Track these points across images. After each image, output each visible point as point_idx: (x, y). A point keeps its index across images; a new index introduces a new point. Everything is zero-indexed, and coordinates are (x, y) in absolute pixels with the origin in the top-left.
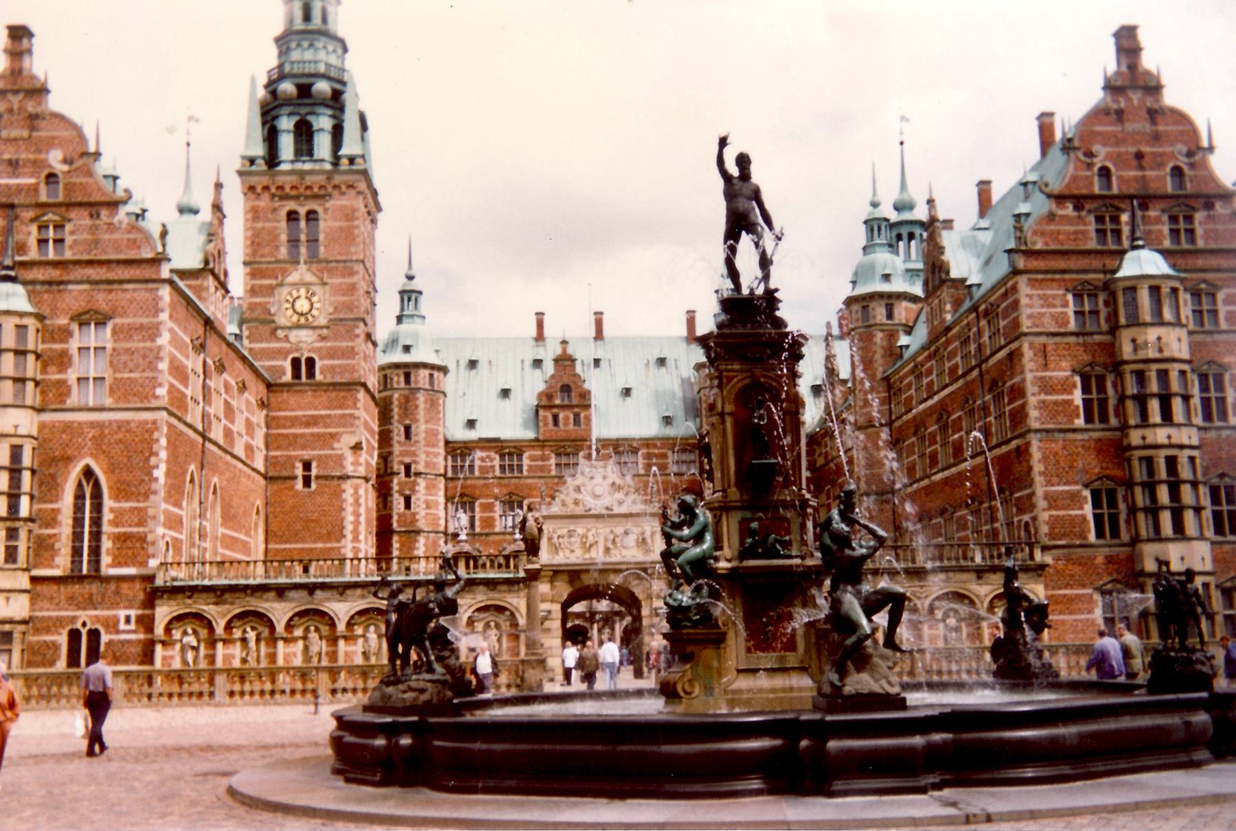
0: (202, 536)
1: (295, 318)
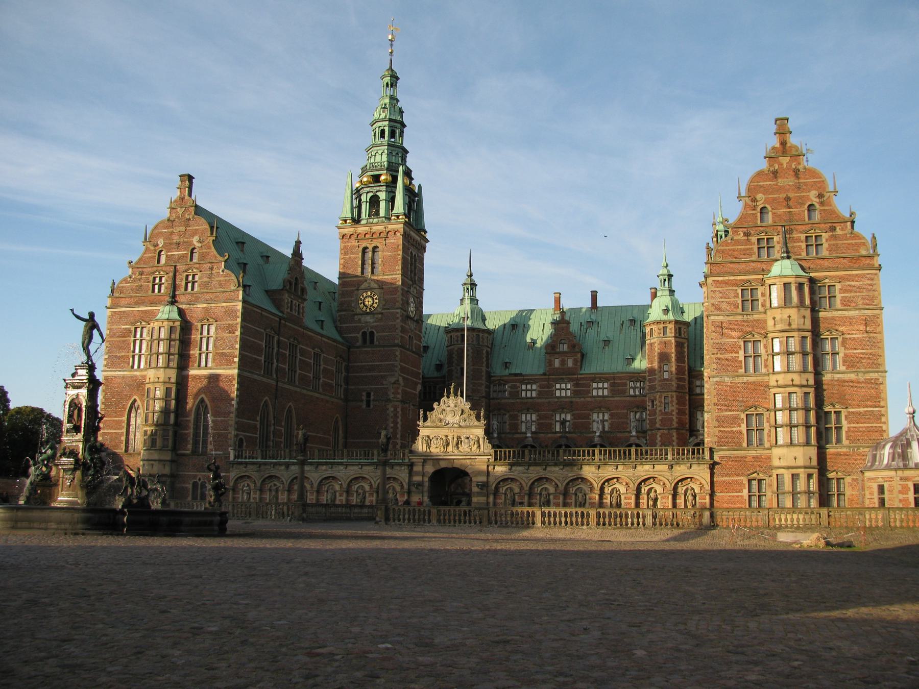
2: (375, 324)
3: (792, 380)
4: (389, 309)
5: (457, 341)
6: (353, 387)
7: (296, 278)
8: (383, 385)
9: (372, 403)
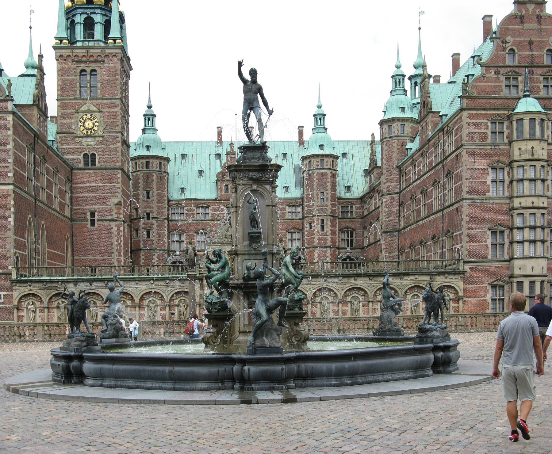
0: (37, 253)
1: (85, 131)
3: (533, 203)
4: (109, 132)
5: (143, 167)
6: (78, 207)
7: (41, 93)
8: (107, 205)
9: (96, 222)
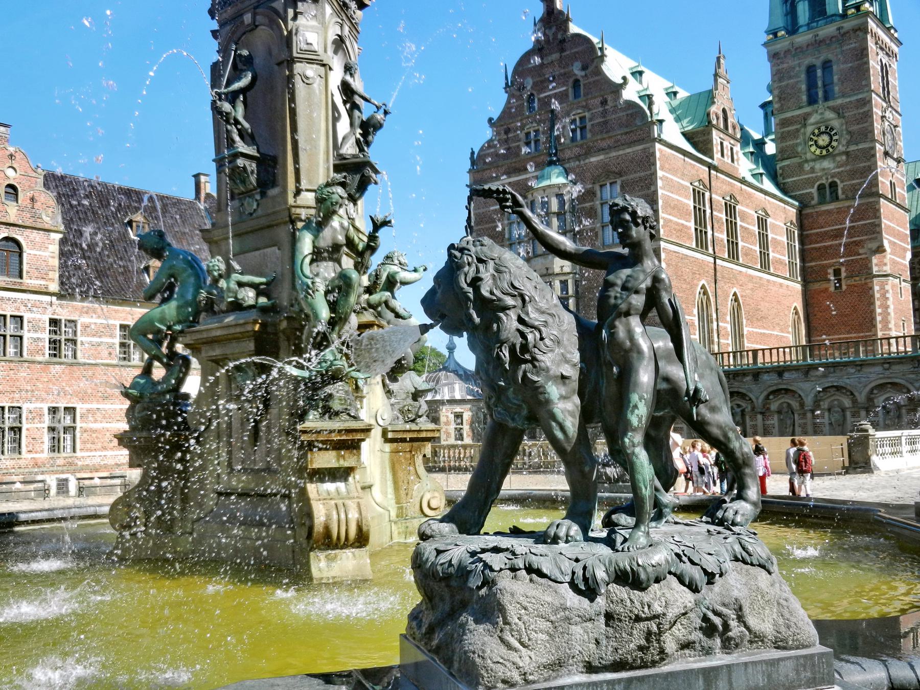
1: (818, 152)
2: (837, 170)
6: (813, 264)
8: (859, 254)
